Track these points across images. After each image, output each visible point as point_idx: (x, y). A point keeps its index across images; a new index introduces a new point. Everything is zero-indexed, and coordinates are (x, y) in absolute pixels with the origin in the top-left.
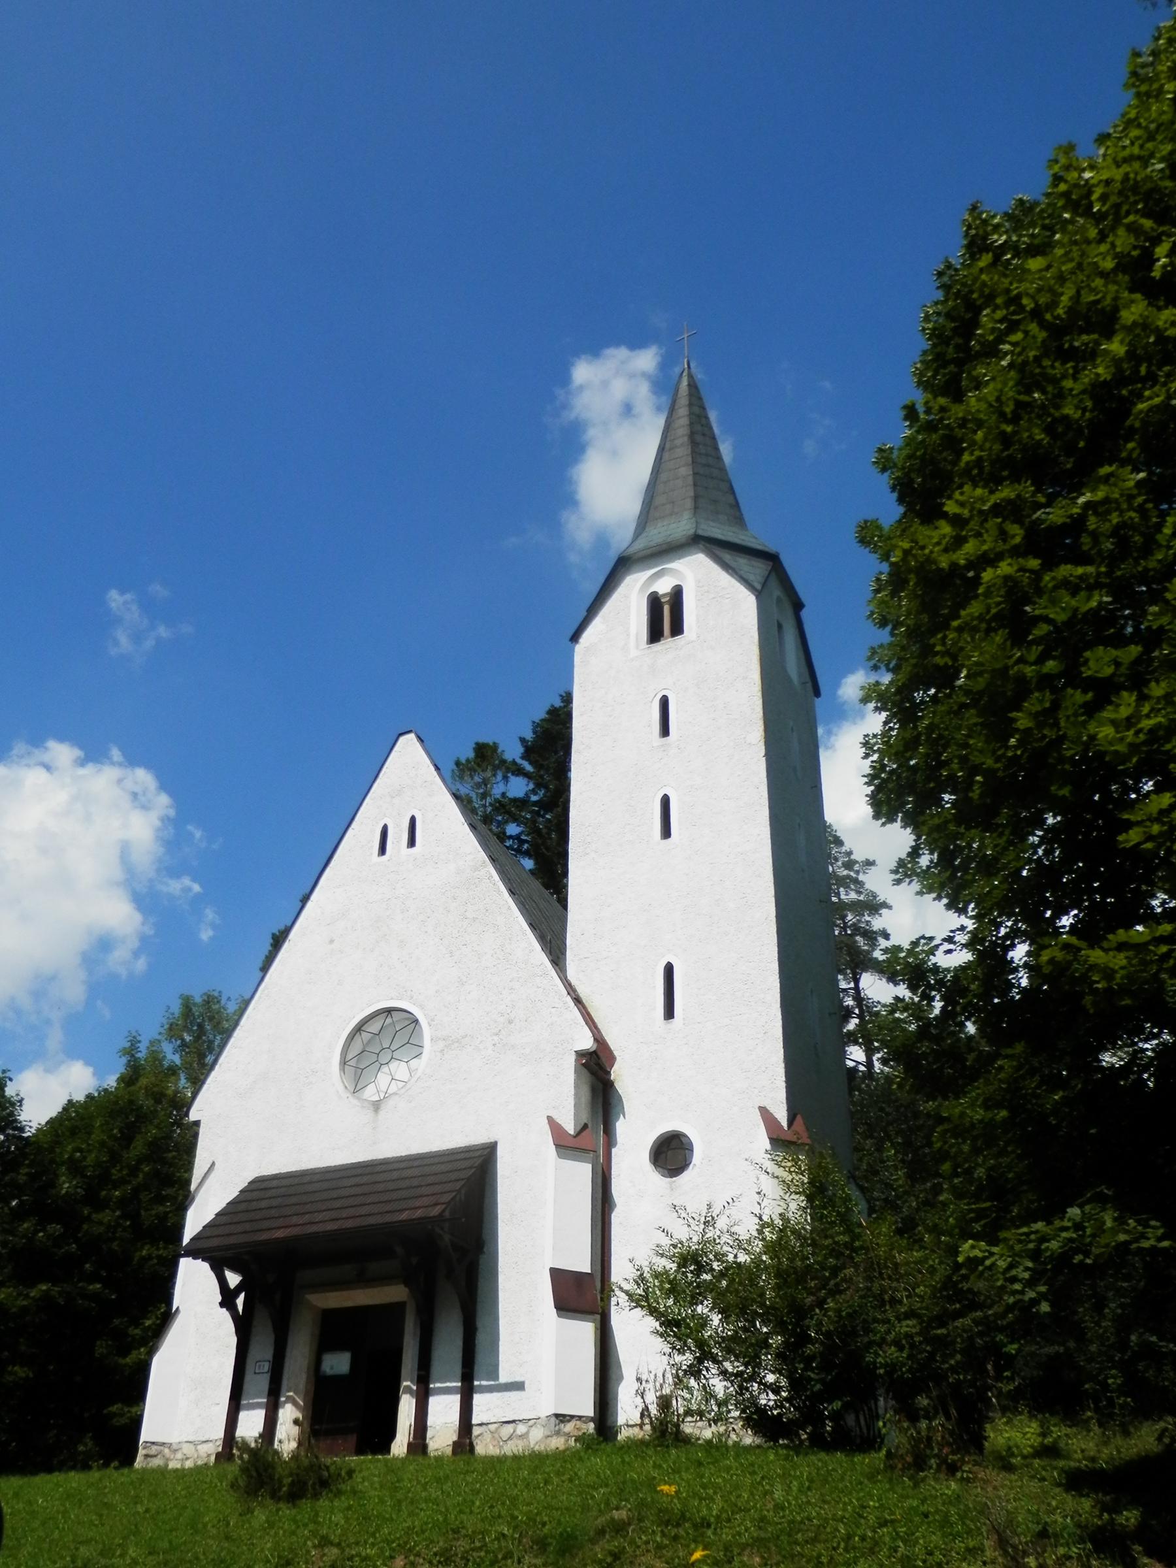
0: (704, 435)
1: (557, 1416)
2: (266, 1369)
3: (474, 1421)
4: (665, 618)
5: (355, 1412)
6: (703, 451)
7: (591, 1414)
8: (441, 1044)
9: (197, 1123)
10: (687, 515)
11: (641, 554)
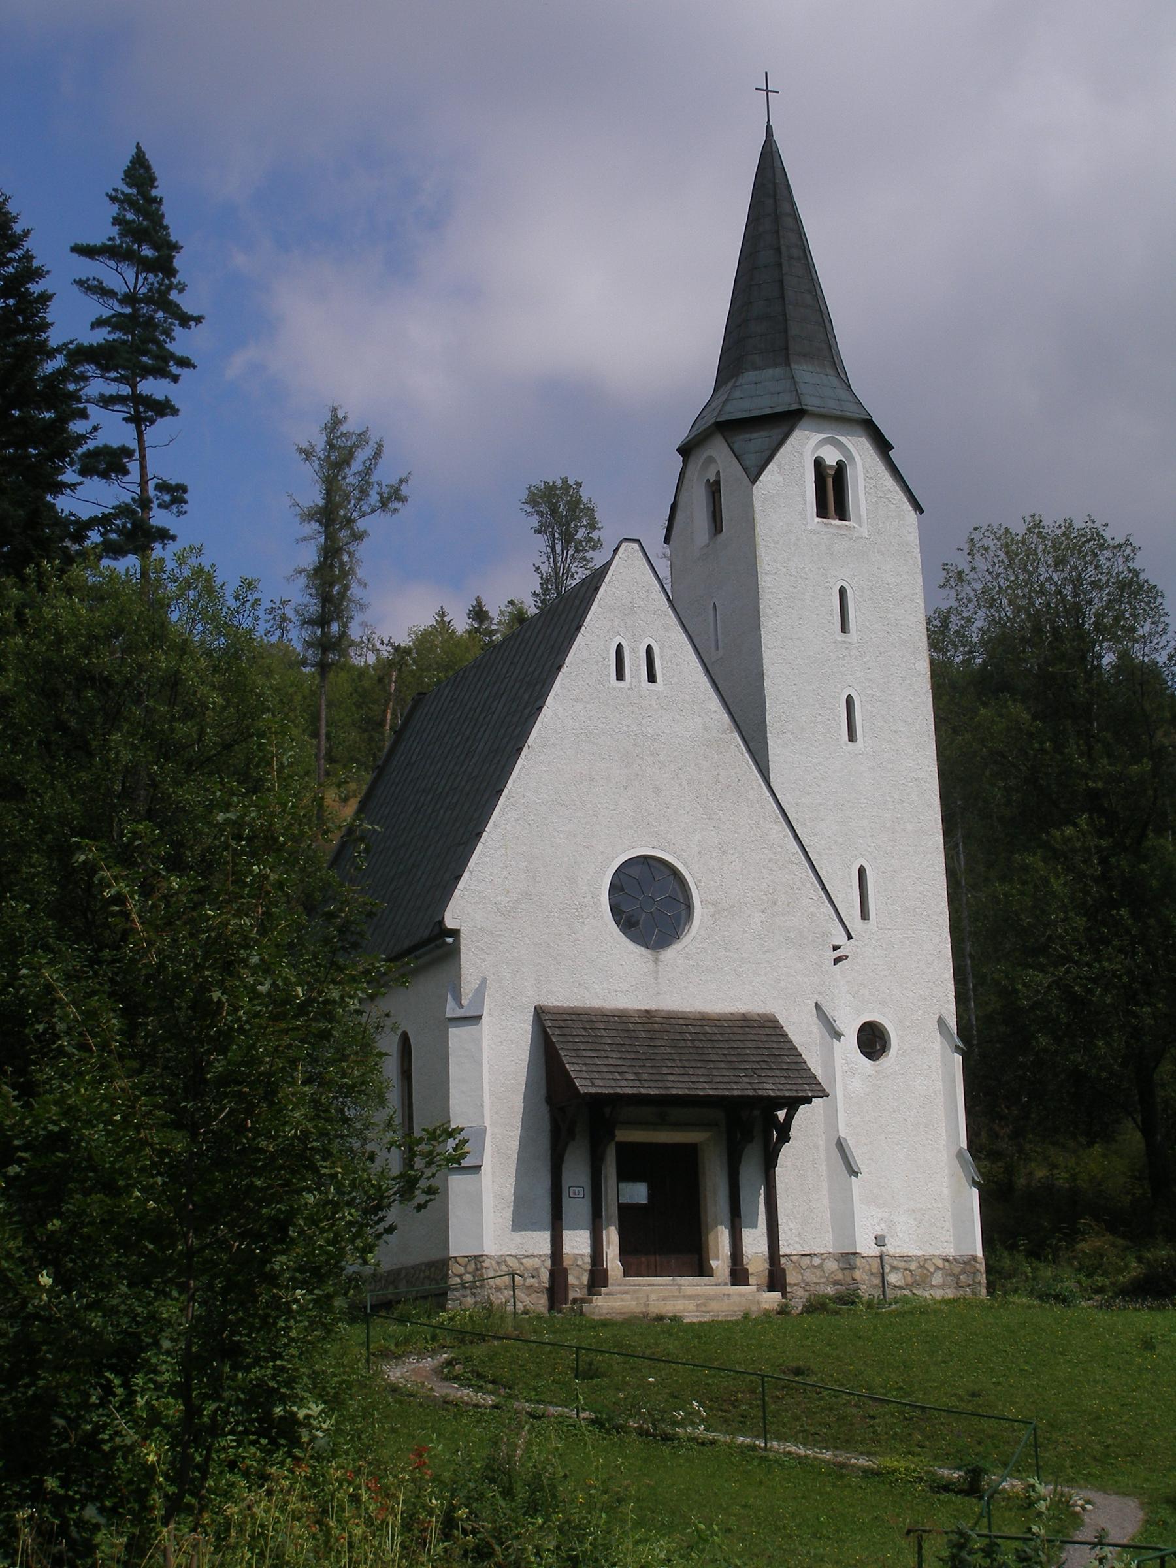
4: (832, 494)
5: (667, 1235)
8: (712, 910)
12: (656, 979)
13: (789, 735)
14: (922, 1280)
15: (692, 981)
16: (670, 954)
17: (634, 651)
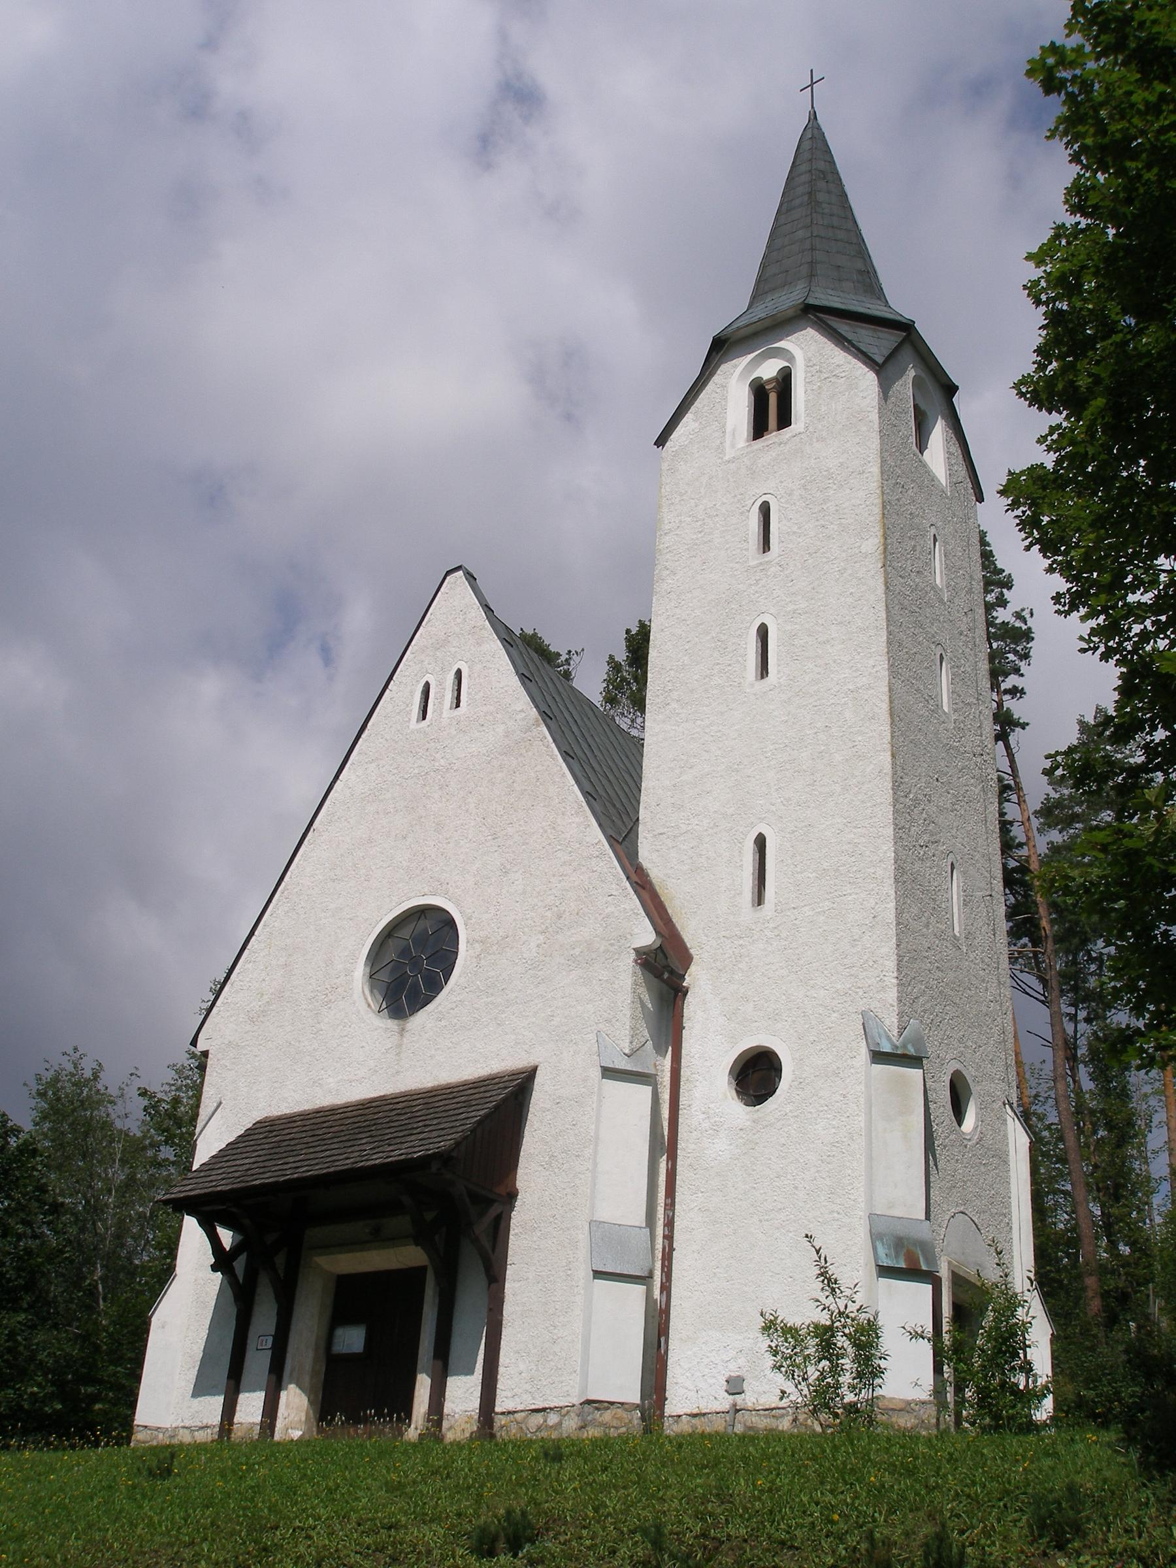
1: (589, 1402)
2: (269, 1345)
3: (498, 1409)
4: (771, 407)
6: (826, 211)
7: (636, 1399)
11: (742, 333)
12: (398, 1054)
13: (674, 705)
15: (442, 1050)
16: (422, 1019)
17: (440, 683)
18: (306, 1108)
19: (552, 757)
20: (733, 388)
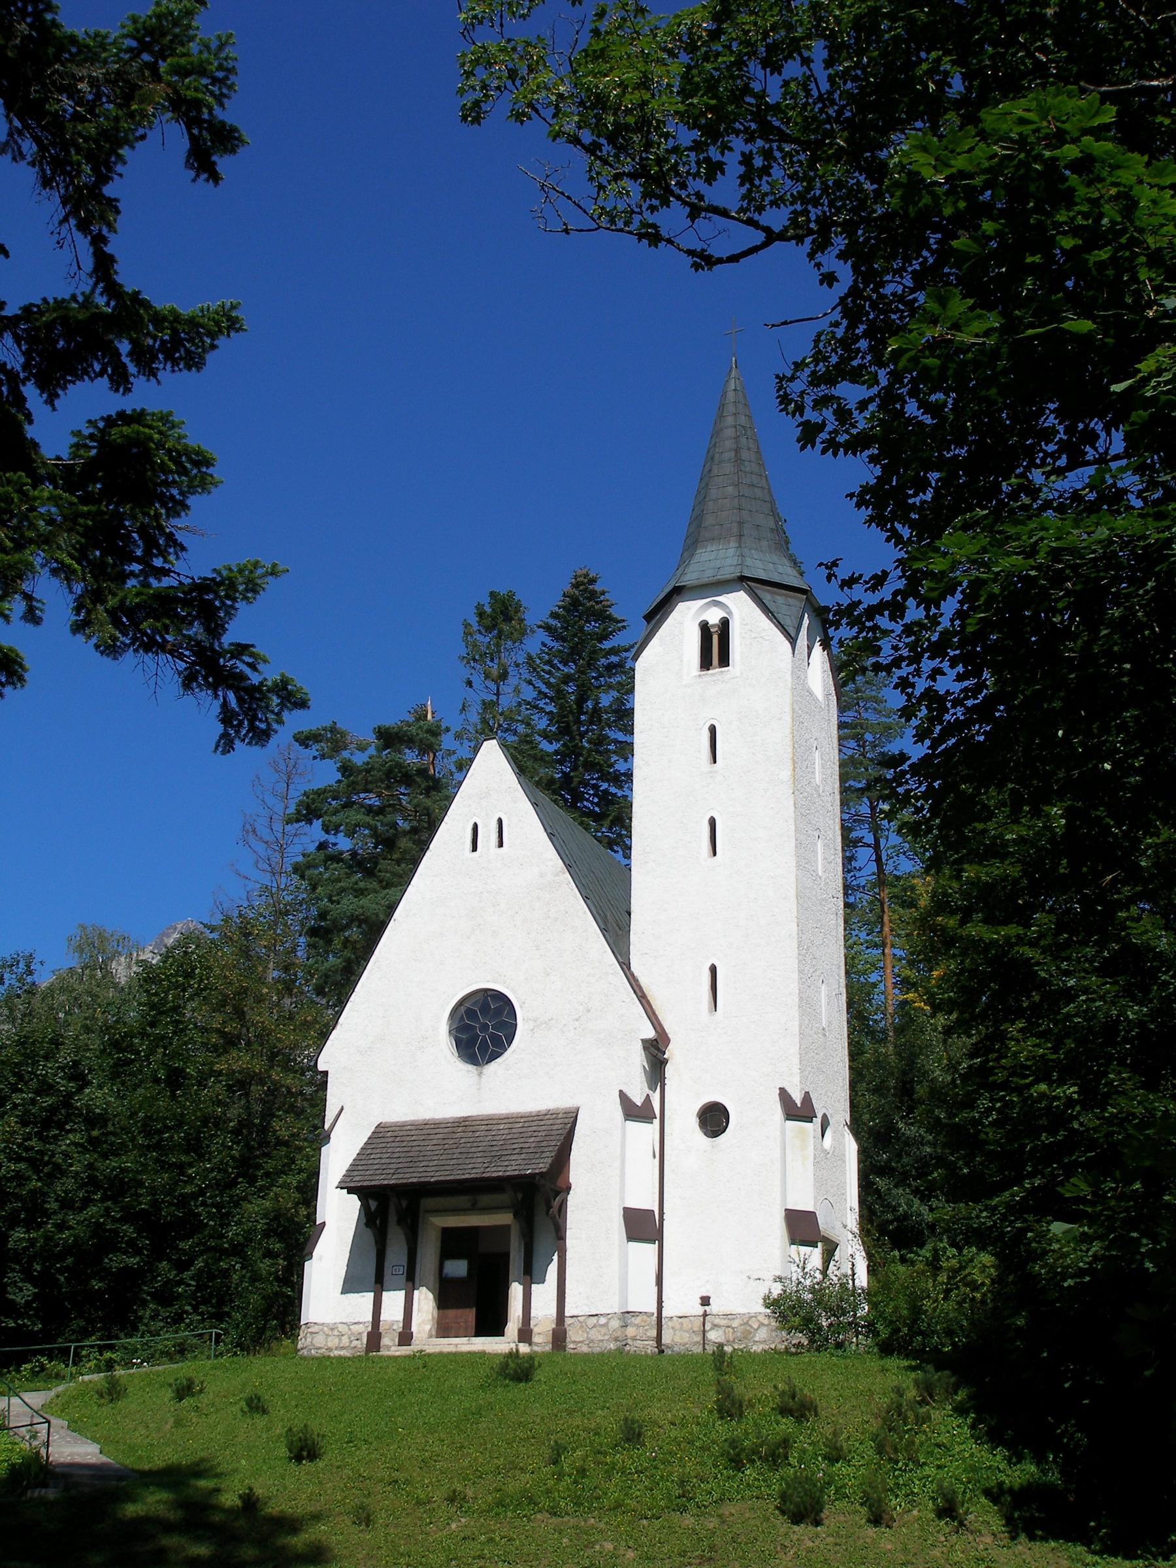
0: (749, 449)
4: (715, 647)
6: (748, 469)
8: (532, 1024)
9: (326, 1073)
10: (733, 544)
14: (747, 1334)
15: (509, 1089)
16: (493, 1065)
18: (412, 1118)
19: (575, 897)
20: (685, 622)
